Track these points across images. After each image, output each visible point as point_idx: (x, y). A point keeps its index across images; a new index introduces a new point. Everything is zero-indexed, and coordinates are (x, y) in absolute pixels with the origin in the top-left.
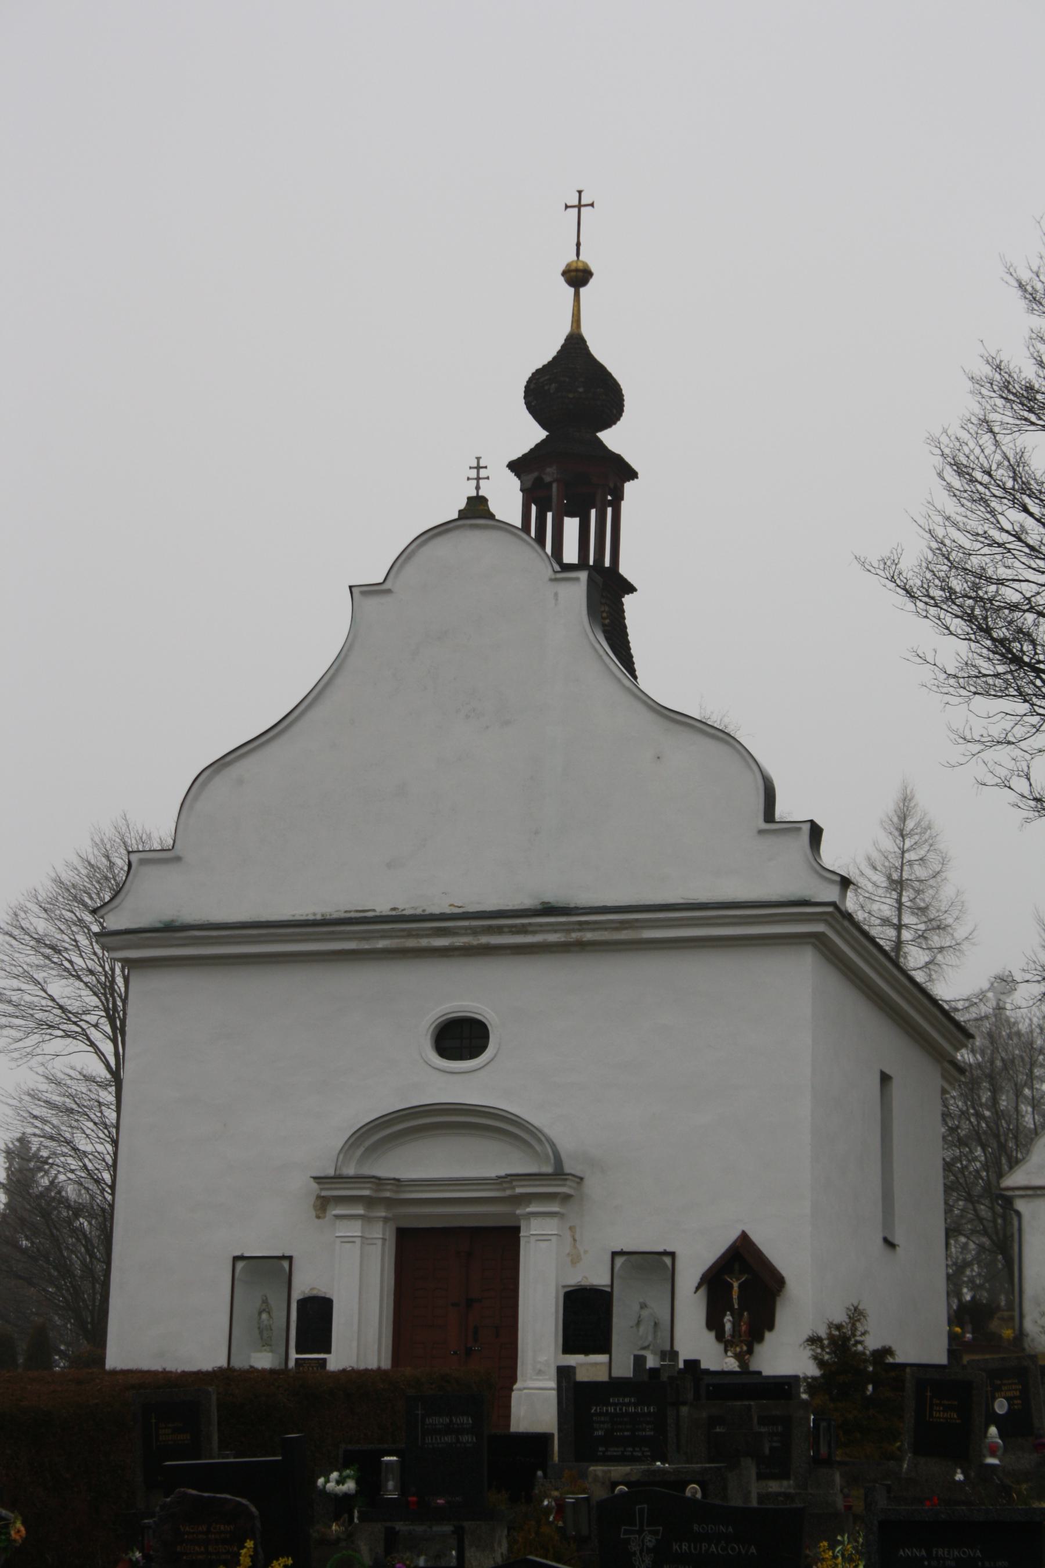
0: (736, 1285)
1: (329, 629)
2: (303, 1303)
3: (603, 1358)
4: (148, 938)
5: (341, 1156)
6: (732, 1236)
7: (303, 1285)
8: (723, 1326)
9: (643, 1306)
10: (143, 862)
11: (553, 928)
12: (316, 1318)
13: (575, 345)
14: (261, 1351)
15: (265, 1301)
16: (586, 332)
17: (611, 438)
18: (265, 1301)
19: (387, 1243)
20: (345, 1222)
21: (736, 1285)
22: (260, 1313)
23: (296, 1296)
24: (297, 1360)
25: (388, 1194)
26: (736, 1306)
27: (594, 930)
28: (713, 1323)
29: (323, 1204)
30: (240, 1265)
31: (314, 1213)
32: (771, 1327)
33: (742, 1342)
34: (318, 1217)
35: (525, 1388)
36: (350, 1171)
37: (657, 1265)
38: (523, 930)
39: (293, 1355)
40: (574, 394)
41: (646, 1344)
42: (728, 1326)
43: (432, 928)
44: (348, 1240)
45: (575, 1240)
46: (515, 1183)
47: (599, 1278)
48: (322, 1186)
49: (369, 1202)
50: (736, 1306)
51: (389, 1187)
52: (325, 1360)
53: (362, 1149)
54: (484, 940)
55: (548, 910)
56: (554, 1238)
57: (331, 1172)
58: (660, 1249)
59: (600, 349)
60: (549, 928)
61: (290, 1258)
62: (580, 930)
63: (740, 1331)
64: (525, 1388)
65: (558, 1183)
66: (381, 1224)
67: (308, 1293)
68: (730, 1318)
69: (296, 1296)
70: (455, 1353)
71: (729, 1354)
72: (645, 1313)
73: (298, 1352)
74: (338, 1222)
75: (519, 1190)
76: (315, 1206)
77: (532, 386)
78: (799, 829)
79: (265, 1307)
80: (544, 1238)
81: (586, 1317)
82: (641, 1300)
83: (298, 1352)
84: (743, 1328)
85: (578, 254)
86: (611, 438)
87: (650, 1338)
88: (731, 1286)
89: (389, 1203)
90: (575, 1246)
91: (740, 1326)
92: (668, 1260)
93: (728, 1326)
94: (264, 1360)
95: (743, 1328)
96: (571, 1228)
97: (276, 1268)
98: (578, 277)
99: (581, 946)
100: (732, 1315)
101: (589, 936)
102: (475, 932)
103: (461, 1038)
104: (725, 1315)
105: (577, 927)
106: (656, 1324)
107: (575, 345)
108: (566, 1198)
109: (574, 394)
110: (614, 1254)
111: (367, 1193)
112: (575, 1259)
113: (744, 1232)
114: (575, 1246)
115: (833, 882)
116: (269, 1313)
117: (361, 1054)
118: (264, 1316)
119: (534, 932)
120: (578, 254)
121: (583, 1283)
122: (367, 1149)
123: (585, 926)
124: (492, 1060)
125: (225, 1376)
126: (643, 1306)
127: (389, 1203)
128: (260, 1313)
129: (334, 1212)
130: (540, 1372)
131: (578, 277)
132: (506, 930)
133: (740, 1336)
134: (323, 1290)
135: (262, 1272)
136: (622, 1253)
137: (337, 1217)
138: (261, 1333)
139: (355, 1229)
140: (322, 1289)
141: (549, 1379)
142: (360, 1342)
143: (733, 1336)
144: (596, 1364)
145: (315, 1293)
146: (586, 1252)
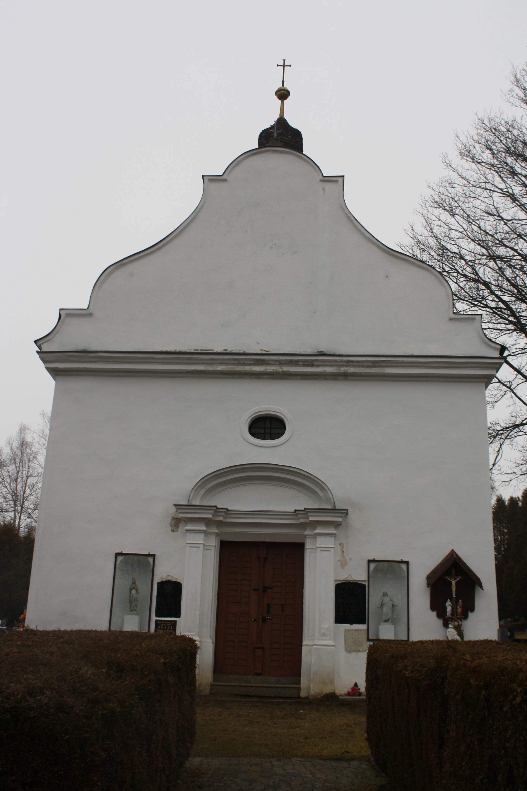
0: (454, 583)
1: (192, 196)
2: (162, 585)
3: (363, 627)
4: (72, 356)
5: (193, 493)
6: (446, 552)
7: (162, 573)
8: (445, 608)
10: (68, 315)
11: (330, 364)
12: (170, 596)
13: (282, 122)
15: (134, 583)
16: (286, 117)
18: (134, 583)
21: (454, 583)
22: (131, 590)
23: (157, 580)
24: (156, 621)
25: (221, 518)
26: (454, 596)
27: (355, 366)
28: (437, 605)
29: (176, 523)
30: (120, 558)
31: (170, 529)
32: (472, 609)
33: (458, 618)
34: (173, 531)
35: (314, 645)
36: (197, 502)
37: (392, 569)
38: (311, 364)
39: (154, 618)
41: (387, 619)
42: (449, 609)
43: (254, 360)
44: (195, 546)
45: (343, 552)
46: (309, 514)
49: (208, 522)
50: (454, 596)
51: (223, 514)
52: (175, 622)
54: (286, 369)
56: (332, 550)
57: (186, 503)
58: (399, 559)
60: (329, 364)
61: (154, 556)
62: (346, 366)
63: (457, 612)
64: (314, 645)
66: (214, 537)
67: (165, 578)
68: (450, 603)
69: (157, 580)
70: (255, 620)
71: (450, 626)
72: (386, 599)
73: (157, 616)
74: (188, 534)
75: (311, 519)
77: (263, 135)
78: (475, 319)
79: (134, 586)
80: (325, 549)
82: (385, 591)
83: (157, 616)
84: (459, 610)
85: (283, 85)
87: (390, 615)
88: (451, 583)
89: (220, 524)
90: (343, 556)
91: (457, 609)
92: (404, 566)
93: (449, 609)
95: (459, 610)
96: (340, 544)
97: (144, 562)
98: (283, 94)
100: (451, 601)
101: (352, 370)
103: (267, 427)
104: (447, 601)
105: (346, 364)
106: (393, 605)
107: (282, 122)
110: (369, 561)
111: (210, 516)
112: (343, 563)
113: (453, 550)
114: (343, 556)
115: (495, 349)
116: (137, 590)
117: (212, 430)
118: (134, 592)
119: (318, 366)
120: (283, 85)
121: (348, 579)
123: (350, 364)
126: (385, 594)
127: (220, 524)
128: (131, 590)
129: (186, 528)
130: (324, 635)
131: (283, 94)
132: (301, 363)
133: (457, 615)
134: (176, 577)
136: (374, 561)
137: (186, 530)
138: (131, 602)
139: (200, 539)
140: (175, 577)
141: (330, 640)
143: (452, 614)
144: (358, 630)
145: (169, 578)
146: (350, 559)
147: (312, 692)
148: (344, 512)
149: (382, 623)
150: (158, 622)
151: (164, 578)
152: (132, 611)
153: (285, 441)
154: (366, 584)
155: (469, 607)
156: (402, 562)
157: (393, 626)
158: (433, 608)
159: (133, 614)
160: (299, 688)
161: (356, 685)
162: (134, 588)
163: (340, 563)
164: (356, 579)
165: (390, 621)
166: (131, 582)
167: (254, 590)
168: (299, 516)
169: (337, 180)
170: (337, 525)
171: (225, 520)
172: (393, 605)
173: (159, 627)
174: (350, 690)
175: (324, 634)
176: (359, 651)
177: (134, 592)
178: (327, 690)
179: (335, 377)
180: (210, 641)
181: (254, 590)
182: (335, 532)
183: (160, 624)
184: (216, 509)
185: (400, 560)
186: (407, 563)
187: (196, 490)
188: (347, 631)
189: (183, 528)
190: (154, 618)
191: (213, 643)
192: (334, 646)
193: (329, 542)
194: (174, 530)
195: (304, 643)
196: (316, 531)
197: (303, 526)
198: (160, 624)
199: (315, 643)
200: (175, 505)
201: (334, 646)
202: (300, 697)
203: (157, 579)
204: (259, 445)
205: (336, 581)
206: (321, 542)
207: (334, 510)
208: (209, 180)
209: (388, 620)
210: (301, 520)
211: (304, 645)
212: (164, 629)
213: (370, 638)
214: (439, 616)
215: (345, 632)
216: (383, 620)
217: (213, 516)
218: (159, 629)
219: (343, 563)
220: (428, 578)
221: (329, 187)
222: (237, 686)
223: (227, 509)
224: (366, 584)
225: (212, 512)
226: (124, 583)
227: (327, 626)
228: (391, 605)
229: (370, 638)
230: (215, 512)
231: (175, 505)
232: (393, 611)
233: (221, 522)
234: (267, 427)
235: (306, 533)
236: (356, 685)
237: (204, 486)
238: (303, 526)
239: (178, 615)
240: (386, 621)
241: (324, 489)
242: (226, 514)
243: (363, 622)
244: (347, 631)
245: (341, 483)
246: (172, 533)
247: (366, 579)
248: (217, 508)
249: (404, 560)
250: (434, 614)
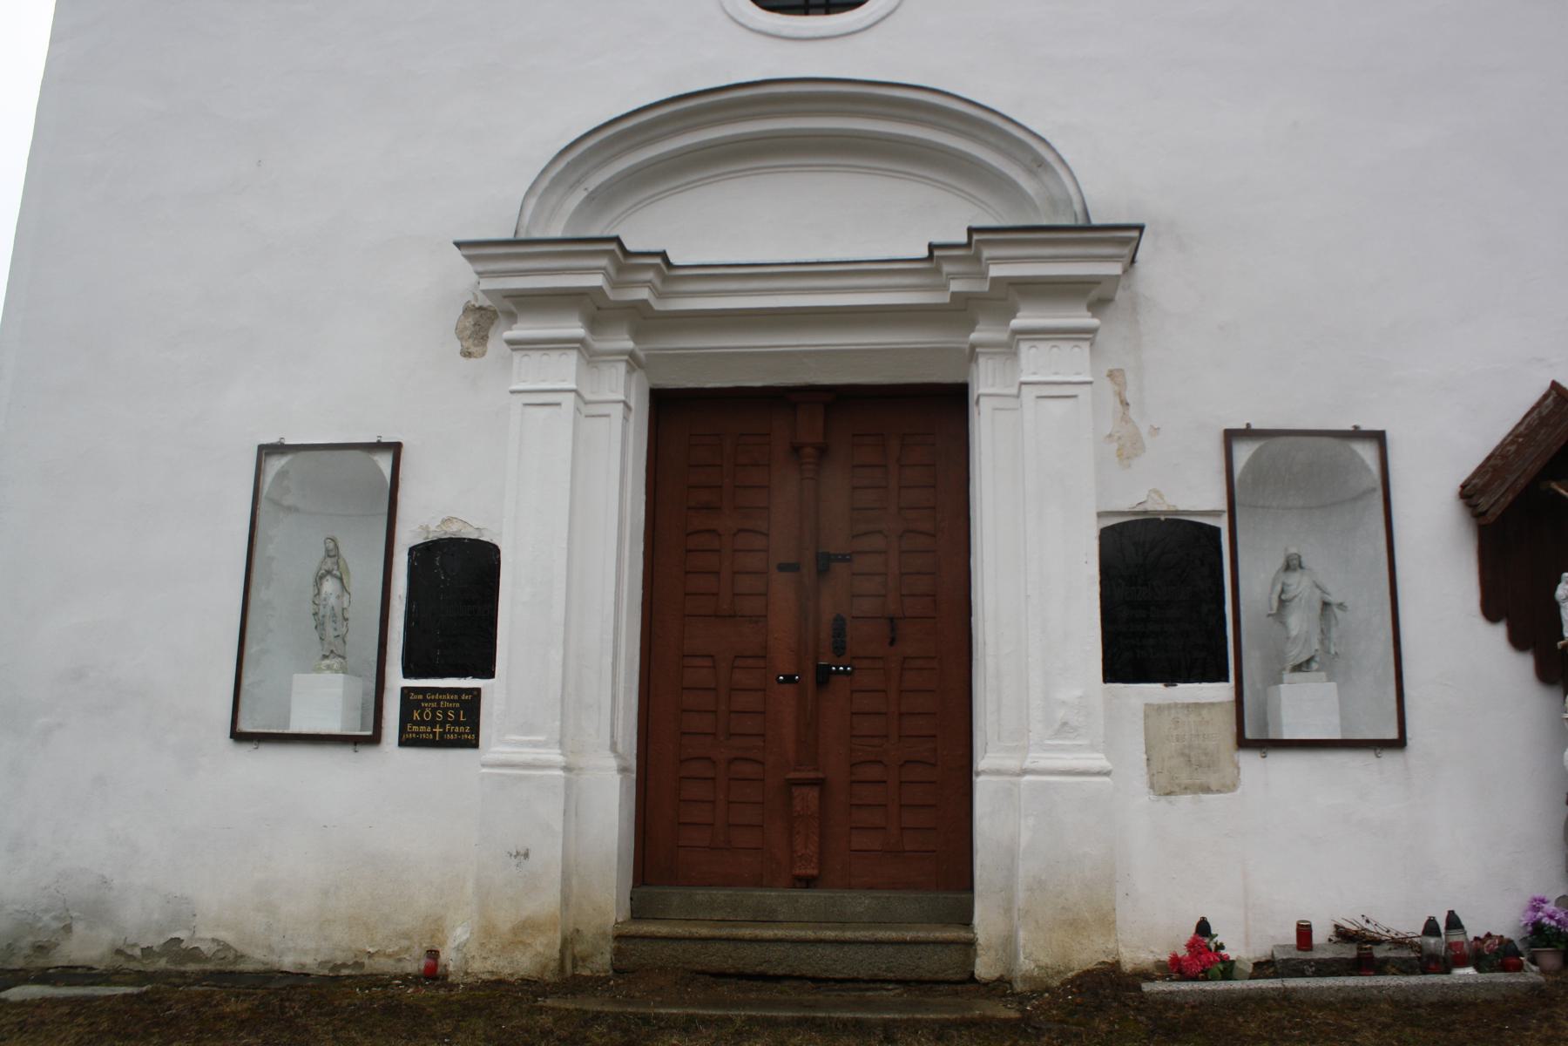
2: (424, 555)
3: (1221, 692)
5: (533, 202)
9: (1292, 565)
14: (318, 670)
15: (333, 553)
18: (333, 553)
19: (632, 418)
20: (535, 357)
22: (319, 579)
24: (405, 692)
25: (643, 294)
29: (480, 322)
30: (275, 465)
31: (457, 346)
34: (467, 354)
35: (1025, 772)
39: (397, 680)
41: (1304, 657)
44: (542, 399)
45: (1125, 404)
46: (987, 253)
47: (1196, 493)
48: (480, 268)
49: (595, 309)
52: (478, 690)
53: (579, 196)
57: (510, 236)
58: (1347, 426)
61: (396, 448)
64: (1025, 772)
66: (622, 367)
67: (436, 532)
70: (789, 679)
72: (1298, 584)
73: (407, 674)
74: (517, 356)
75: (996, 271)
76: (459, 332)
79: (333, 566)
82: (1293, 550)
83: (407, 674)
89: (642, 320)
90: (1125, 419)
96: (1111, 375)
106: (1326, 605)
110: (1231, 436)
111: (597, 280)
114: (1125, 419)
116: (341, 579)
118: (329, 586)
121: (1150, 507)
122: (591, 198)
124: (883, 18)
126: (1292, 565)
127: (642, 320)
128: (319, 579)
129: (509, 334)
134: (476, 524)
136: (1248, 433)
137: (511, 342)
138: (320, 626)
139: (563, 370)
140: (473, 523)
141: (1092, 748)
144: (1198, 706)
145: (454, 530)
146: (1155, 431)
147: (1025, 965)
148: (1125, 237)
149: (1287, 676)
150: (413, 697)
151: (432, 528)
152: (325, 657)
153: (883, 13)
154: (1223, 524)
156: (1357, 434)
157: (1333, 685)
158: (1492, 609)
159: (329, 668)
160: (970, 944)
161: (1203, 928)
162: (329, 572)
163: (1115, 446)
164: (1181, 508)
165: (1314, 665)
166: (322, 553)
167: (782, 568)
168: (947, 268)
171: (659, 306)
172: (1326, 605)
173: (416, 715)
174: (1182, 952)
175: (1065, 724)
176: (1207, 790)
177: (329, 586)
178: (1087, 954)
180: (612, 763)
181: (782, 568)
182: (1094, 322)
183: (417, 705)
184: (624, 258)
185: (1348, 427)
186: (1379, 438)
187: (546, 190)
188: (1153, 711)
190: (397, 680)
191: (623, 770)
192: (1107, 774)
193: (1069, 362)
194: (473, 349)
195: (982, 762)
196: (1016, 323)
197: (962, 311)
198: (417, 705)
199: (1028, 764)
200: (459, 245)
201: (1107, 774)
202: (972, 978)
203: (408, 536)
204: (785, 33)
205: (1100, 515)
206: (1036, 361)
207: (1085, 232)
209: (1308, 661)
210: (956, 286)
211: (984, 772)
212: (433, 723)
213: (1249, 735)
214: (1518, 641)
215: (1146, 716)
216: (1289, 666)
217: (615, 285)
218: (418, 723)
219: (1128, 448)
220: (1468, 493)
222: (720, 939)
223: (663, 255)
224: (1223, 524)
225: (603, 262)
226: (294, 552)
227: (1078, 692)
228: (1318, 606)
229: (1249, 735)
230: (621, 269)
231: (459, 245)
232: (1325, 634)
233: (640, 308)
235: (974, 336)
236: (1203, 928)
237: (579, 182)
238: (962, 311)
239: (488, 671)
240: (1298, 668)
241: (1041, 163)
242: (666, 279)
243: (1216, 673)
244: (1153, 711)
246: (464, 360)
247: (1221, 504)
248: (627, 253)
249: (1366, 426)
250: (1500, 632)
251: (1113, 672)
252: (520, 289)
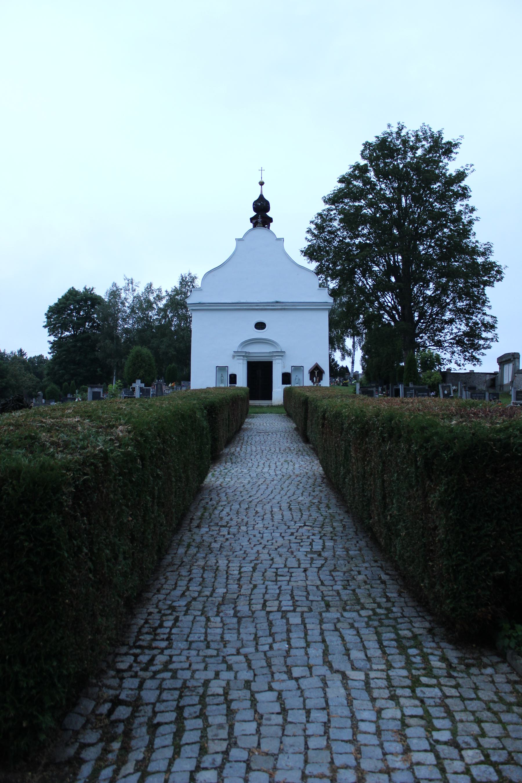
1: (232, 247)
2: (230, 375)
7: (230, 372)
12: (233, 378)
13: (261, 197)
17: (269, 214)
28: (311, 379)
29: (234, 357)
37: (298, 369)
38: (274, 306)
40: (261, 207)
47: (289, 371)
49: (243, 356)
55: (277, 302)
59: (266, 197)
65: (281, 354)
79: (222, 376)
81: (286, 378)
86: (269, 214)
89: (247, 357)
94: (222, 385)
98: (262, 184)
99: (284, 309)
102: (264, 306)
107: (261, 197)
108: (282, 356)
109: (261, 207)
112: (284, 367)
125: (216, 388)
127: (247, 357)
131: (262, 184)
135: (221, 369)
139: (241, 361)
142: (242, 382)
155: (321, 379)
158: (310, 379)
169: (282, 240)
170: (282, 356)
179: (281, 309)
189: (236, 358)
193: (280, 361)
197: (272, 356)
206: (277, 361)
208: (238, 240)
221: (279, 242)
226: (219, 376)
234: (260, 326)
238: (272, 356)
245: (283, 344)
251: (283, 383)
252: (237, 354)
